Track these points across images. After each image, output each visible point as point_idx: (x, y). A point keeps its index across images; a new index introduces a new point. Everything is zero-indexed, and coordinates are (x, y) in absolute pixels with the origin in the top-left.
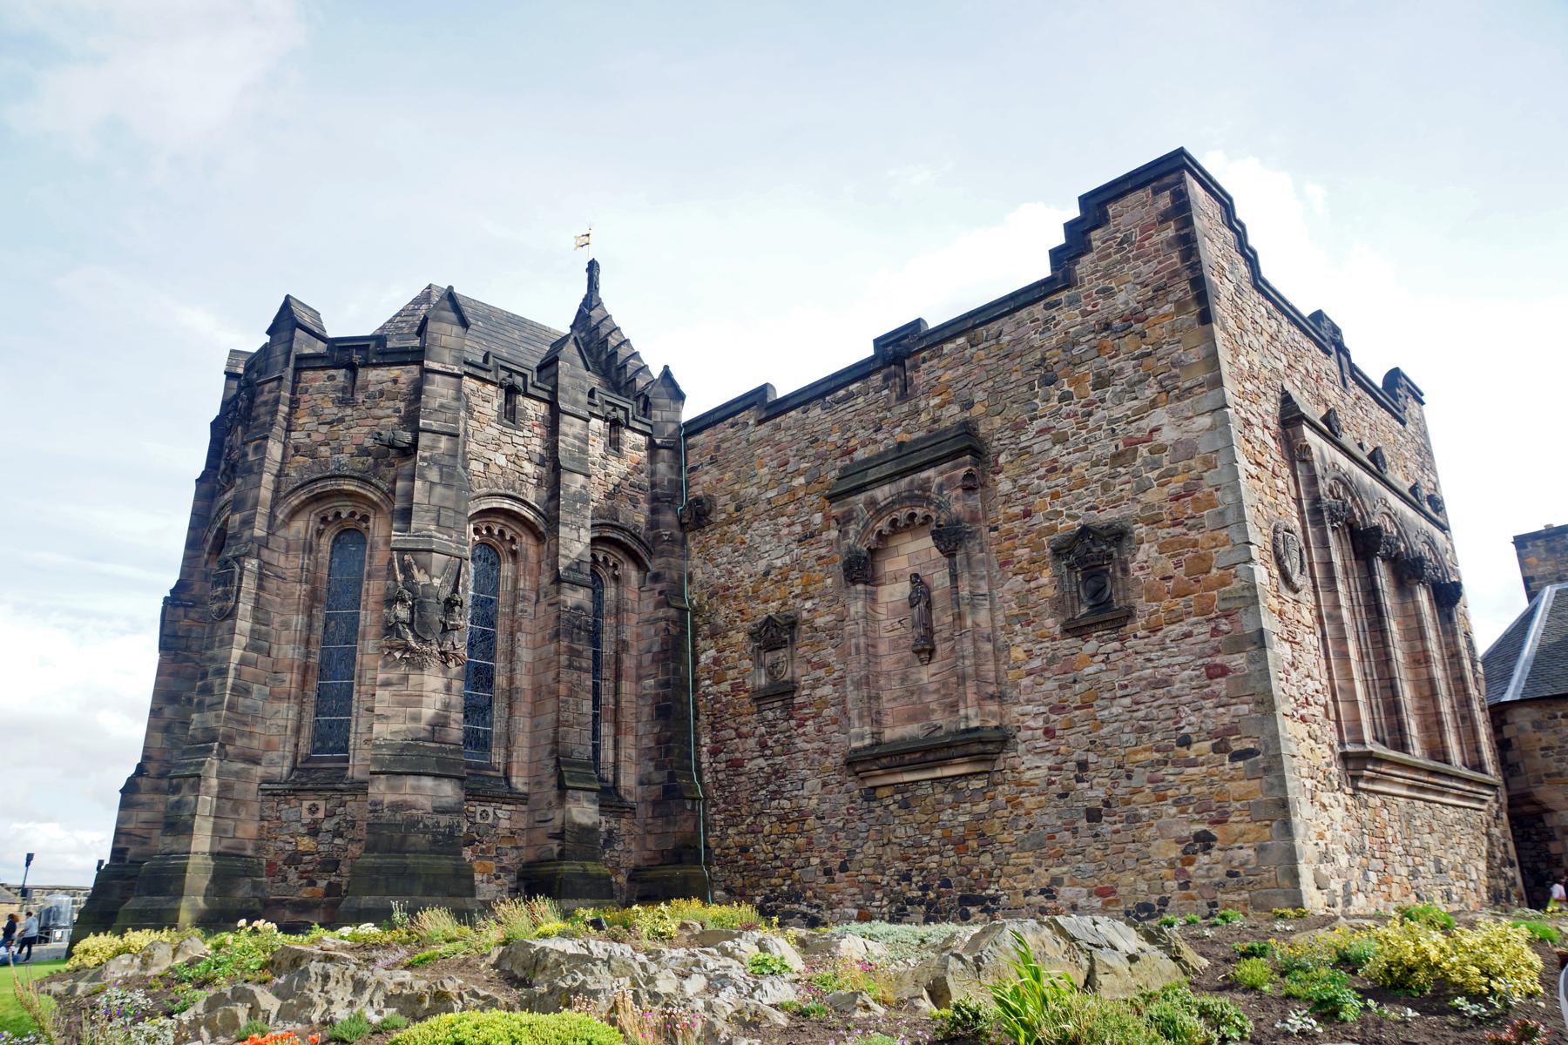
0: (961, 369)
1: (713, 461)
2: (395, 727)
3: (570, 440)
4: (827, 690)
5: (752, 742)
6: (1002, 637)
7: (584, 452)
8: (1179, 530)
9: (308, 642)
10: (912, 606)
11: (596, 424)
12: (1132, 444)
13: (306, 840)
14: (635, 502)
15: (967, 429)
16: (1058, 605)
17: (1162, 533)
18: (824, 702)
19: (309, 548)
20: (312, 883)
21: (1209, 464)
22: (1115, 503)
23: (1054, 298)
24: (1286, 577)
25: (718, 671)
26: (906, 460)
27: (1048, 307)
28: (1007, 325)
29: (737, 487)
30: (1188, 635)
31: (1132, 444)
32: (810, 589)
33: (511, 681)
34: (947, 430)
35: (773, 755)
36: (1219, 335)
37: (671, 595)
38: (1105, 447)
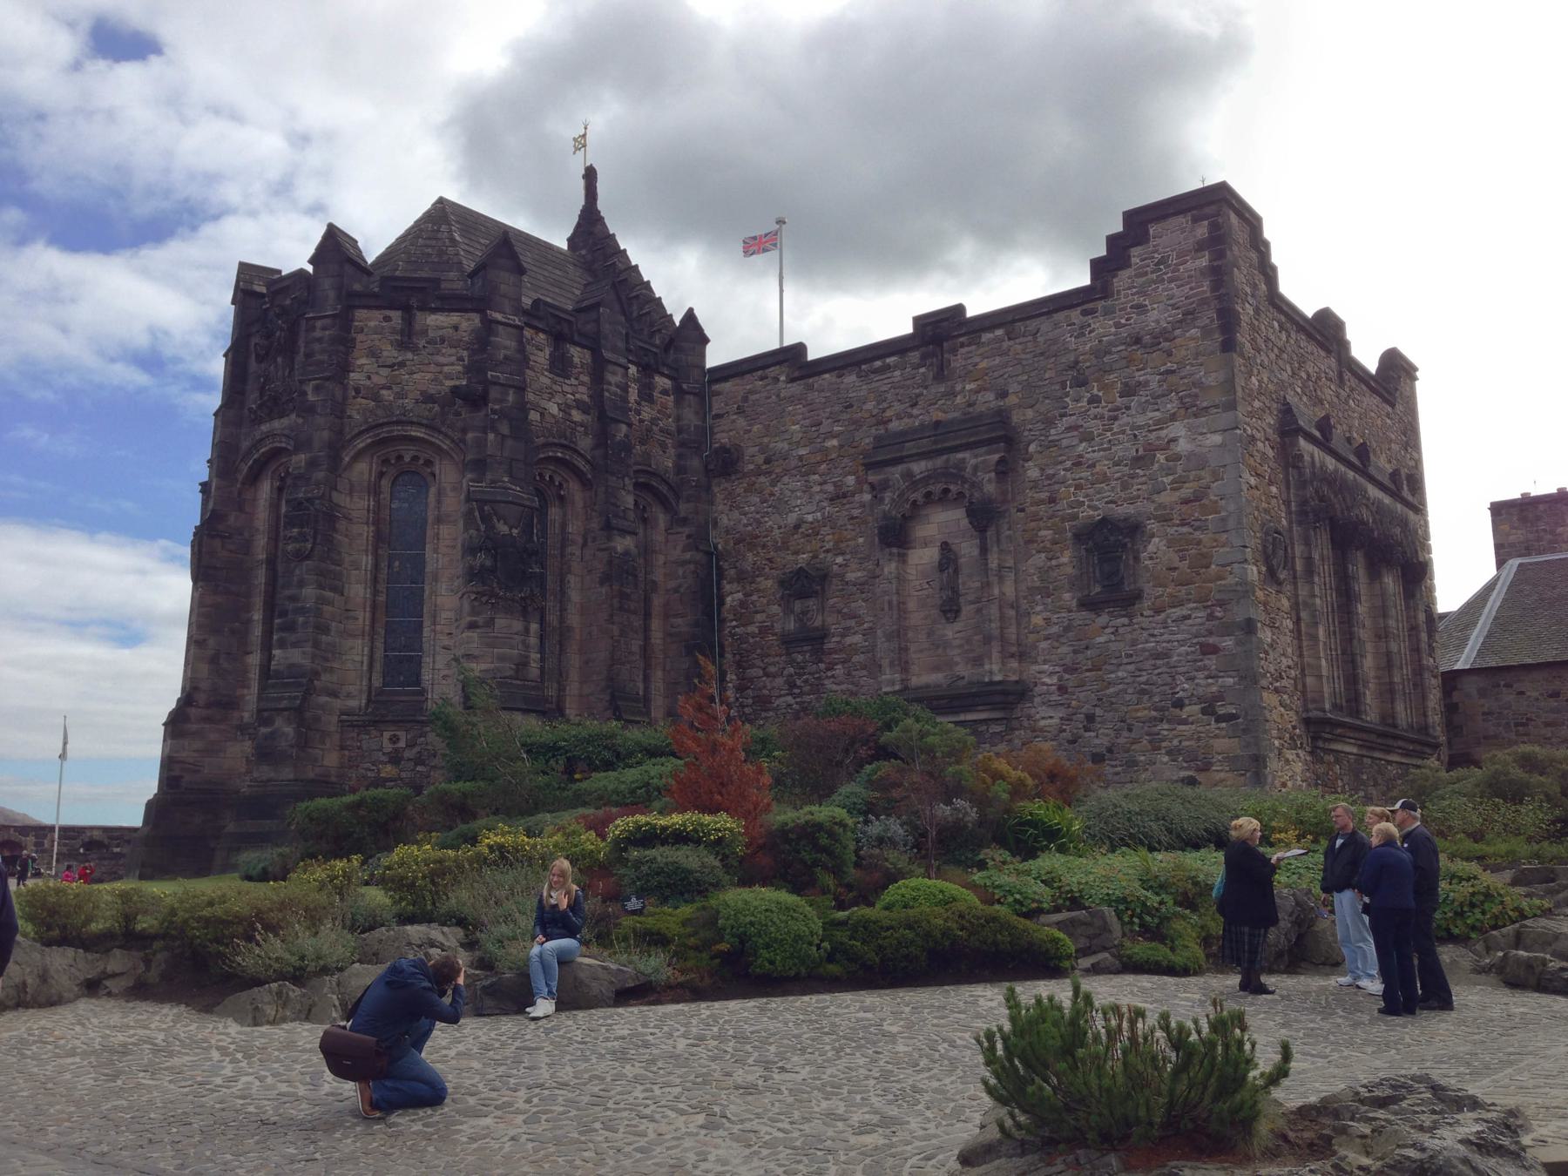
0: (997, 360)
1: (740, 411)
2: (483, 666)
3: (613, 388)
4: (857, 638)
5: (780, 681)
6: (1024, 604)
7: (625, 400)
8: (1185, 529)
9: (375, 580)
10: (942, 571)
11: (633, 370)
12: (1151, 450)
13: (389, 768)
14: (663, 447)
15: (1002, 417)
17: (1171, 531)
18: (854, 649)
19: (374, 490)
21: (1216, 477)
22: (1132, 500)
23: (1090, 306)
24: (1271, 575)
25: (745, 612)
26: (942, 439)
27: (1085, 313)
28: (1044, 325)
29: (766, 440)
30: (1188, 617)
31: (1151, 450)
32: (842, 545)
33: (562, 620)
35: (801, 694)
36: (1239, 361)
37: (699, 540)
38: (1126, 450)
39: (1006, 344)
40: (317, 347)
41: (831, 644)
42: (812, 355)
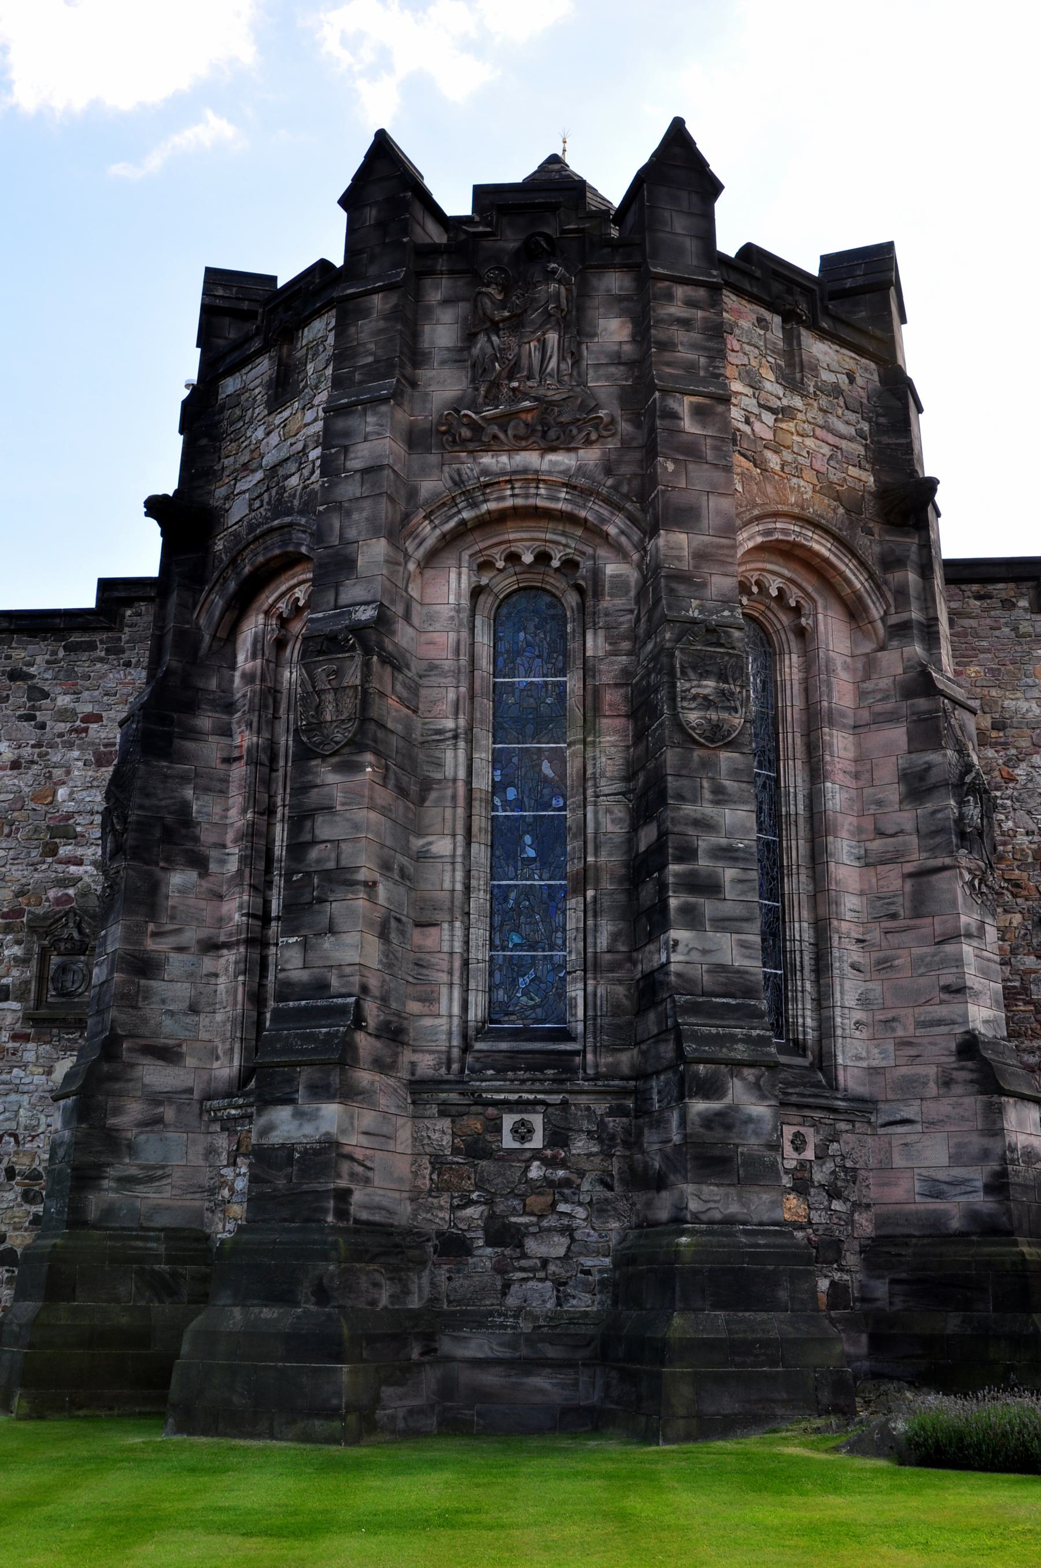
13: (792, 1201)
29: (993, 693)
40: (680, 335)
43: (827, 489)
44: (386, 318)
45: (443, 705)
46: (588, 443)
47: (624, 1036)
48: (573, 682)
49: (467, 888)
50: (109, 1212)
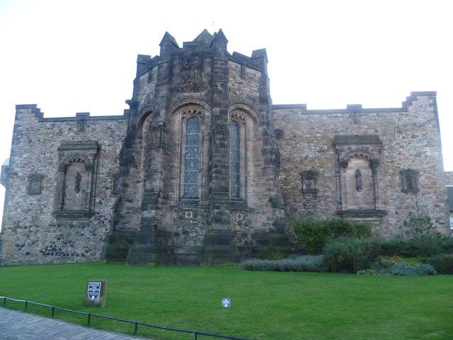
0: (374, 122)
4: (329, 194)
13: (238, 227)
16: (401, 184)
18: (328, 197)
20: (240, 241)
22: (416, 165)
34: (371, 136)
39: (377, 118)
40: (218, 70)
41: (318, 195)
42: (309, 108)
43: (249, 98)
44: (167, 68)
45: (177, 139)
46: (202, 91)
47: (206, 198)
48: (200, 135)
49: (180, 172)
50: (120, 228)
